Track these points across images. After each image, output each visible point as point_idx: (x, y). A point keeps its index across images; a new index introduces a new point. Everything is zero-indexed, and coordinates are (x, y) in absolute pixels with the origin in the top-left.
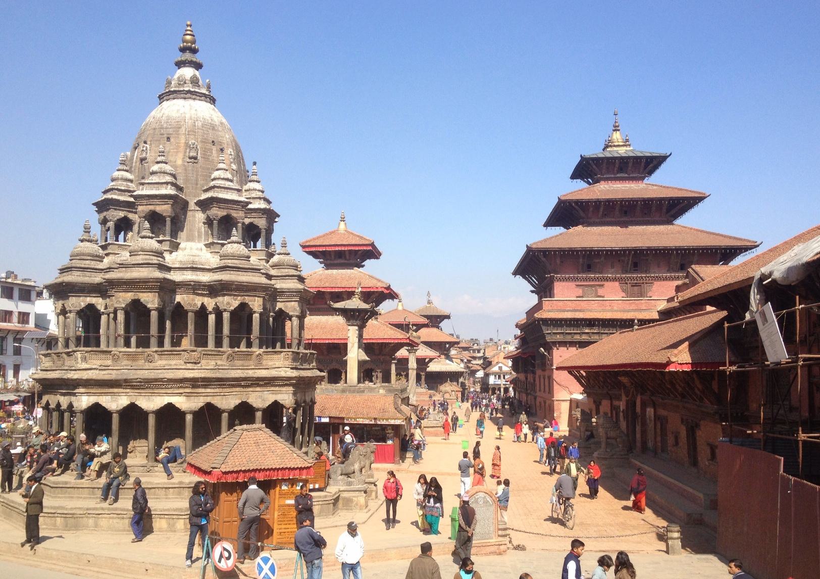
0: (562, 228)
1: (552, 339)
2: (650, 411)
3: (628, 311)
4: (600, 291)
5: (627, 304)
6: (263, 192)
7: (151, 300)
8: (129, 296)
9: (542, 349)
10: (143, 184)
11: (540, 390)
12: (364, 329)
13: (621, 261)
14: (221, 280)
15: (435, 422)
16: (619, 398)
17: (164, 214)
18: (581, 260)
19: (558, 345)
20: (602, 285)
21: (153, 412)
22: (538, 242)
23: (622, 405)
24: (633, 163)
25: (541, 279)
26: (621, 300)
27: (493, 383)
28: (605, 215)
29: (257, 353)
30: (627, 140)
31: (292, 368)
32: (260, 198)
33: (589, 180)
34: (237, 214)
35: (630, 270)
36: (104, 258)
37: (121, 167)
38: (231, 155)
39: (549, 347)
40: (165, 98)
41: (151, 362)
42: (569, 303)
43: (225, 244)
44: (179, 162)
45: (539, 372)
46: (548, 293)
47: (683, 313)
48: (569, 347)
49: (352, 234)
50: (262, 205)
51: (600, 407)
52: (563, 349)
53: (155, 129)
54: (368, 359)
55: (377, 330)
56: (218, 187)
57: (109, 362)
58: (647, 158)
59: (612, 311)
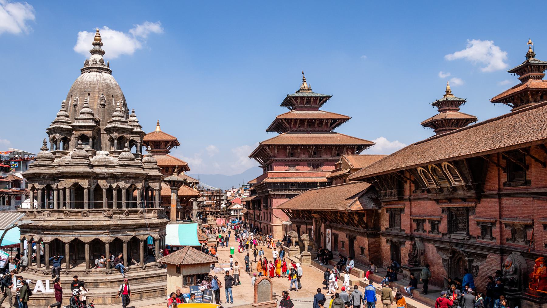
3: (312, 178)
6: (138, 122)
7: (84, 183)
8: (73, 181)
10: (77, 119)
11: (264, 219)
14: (122, 172)
15: (212, 239)
16: (311, 224)
17: (89, 136)
18: (288, 151)
21: (88, 243)
24: (314, 100)
28: (300, 126)
29: (140, 211)
30: (310, 87)
31: (158, 218)
32: (137, 126)
33: (291, 107)
34: (128, 136)
36: (54, 159)
37: (63, 109)
38: (122, 102)
40: (85, 71)
41: (86, 217)
43: (121, 152)
44: (95, 107)
46: (270, 168)
50: (139, 130)
53: (81, 88)
55: (184, 191)
56: (117, 121)
57: (63, 217)
58: (321, 97)
59: (304, 177)
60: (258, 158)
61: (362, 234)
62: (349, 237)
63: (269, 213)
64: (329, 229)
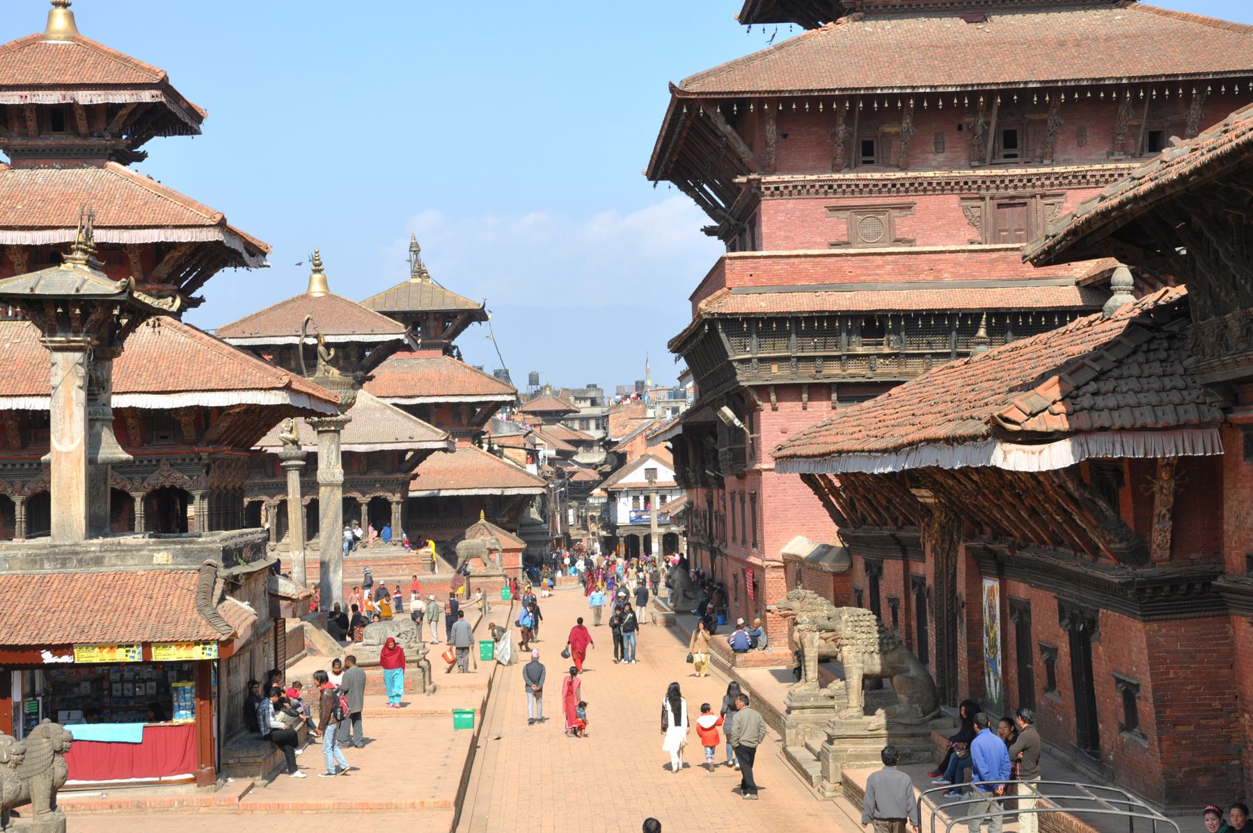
0: (795, 25)
1: (756, 378)
2: (990, 585)
4: (904, 224)
5: (982, 262)
9: (727, 411)
11: (734, 539)
12: (115, 361)
13: (964, 127)
18: (841, 130)
19: (773, 398)
20: (909, 207)
22: (708, 74)
23: (925, 569)
25: (729, 191)
26: (964, 251)
27: (627, 522)
35: (993, 158)
39: (745, 403)
42: (806, 264)
45: (730, 481)
47: (1147, 287)
48: (810, 399)
49: (95, 48)
51: (881, 582)
52: (789, 407)
54: (125, 456)
59: (937, 284)
60: (694, 179)
61: (1112, 594)
62: (1074, 621)
63: (747, 498)
64: (990, 576)
